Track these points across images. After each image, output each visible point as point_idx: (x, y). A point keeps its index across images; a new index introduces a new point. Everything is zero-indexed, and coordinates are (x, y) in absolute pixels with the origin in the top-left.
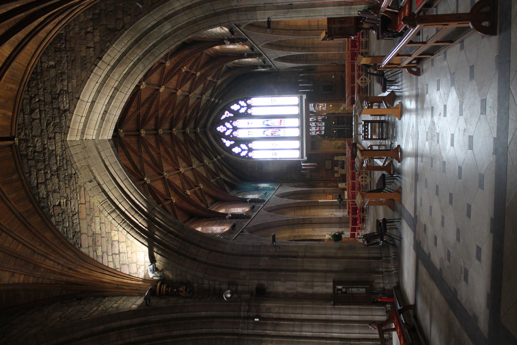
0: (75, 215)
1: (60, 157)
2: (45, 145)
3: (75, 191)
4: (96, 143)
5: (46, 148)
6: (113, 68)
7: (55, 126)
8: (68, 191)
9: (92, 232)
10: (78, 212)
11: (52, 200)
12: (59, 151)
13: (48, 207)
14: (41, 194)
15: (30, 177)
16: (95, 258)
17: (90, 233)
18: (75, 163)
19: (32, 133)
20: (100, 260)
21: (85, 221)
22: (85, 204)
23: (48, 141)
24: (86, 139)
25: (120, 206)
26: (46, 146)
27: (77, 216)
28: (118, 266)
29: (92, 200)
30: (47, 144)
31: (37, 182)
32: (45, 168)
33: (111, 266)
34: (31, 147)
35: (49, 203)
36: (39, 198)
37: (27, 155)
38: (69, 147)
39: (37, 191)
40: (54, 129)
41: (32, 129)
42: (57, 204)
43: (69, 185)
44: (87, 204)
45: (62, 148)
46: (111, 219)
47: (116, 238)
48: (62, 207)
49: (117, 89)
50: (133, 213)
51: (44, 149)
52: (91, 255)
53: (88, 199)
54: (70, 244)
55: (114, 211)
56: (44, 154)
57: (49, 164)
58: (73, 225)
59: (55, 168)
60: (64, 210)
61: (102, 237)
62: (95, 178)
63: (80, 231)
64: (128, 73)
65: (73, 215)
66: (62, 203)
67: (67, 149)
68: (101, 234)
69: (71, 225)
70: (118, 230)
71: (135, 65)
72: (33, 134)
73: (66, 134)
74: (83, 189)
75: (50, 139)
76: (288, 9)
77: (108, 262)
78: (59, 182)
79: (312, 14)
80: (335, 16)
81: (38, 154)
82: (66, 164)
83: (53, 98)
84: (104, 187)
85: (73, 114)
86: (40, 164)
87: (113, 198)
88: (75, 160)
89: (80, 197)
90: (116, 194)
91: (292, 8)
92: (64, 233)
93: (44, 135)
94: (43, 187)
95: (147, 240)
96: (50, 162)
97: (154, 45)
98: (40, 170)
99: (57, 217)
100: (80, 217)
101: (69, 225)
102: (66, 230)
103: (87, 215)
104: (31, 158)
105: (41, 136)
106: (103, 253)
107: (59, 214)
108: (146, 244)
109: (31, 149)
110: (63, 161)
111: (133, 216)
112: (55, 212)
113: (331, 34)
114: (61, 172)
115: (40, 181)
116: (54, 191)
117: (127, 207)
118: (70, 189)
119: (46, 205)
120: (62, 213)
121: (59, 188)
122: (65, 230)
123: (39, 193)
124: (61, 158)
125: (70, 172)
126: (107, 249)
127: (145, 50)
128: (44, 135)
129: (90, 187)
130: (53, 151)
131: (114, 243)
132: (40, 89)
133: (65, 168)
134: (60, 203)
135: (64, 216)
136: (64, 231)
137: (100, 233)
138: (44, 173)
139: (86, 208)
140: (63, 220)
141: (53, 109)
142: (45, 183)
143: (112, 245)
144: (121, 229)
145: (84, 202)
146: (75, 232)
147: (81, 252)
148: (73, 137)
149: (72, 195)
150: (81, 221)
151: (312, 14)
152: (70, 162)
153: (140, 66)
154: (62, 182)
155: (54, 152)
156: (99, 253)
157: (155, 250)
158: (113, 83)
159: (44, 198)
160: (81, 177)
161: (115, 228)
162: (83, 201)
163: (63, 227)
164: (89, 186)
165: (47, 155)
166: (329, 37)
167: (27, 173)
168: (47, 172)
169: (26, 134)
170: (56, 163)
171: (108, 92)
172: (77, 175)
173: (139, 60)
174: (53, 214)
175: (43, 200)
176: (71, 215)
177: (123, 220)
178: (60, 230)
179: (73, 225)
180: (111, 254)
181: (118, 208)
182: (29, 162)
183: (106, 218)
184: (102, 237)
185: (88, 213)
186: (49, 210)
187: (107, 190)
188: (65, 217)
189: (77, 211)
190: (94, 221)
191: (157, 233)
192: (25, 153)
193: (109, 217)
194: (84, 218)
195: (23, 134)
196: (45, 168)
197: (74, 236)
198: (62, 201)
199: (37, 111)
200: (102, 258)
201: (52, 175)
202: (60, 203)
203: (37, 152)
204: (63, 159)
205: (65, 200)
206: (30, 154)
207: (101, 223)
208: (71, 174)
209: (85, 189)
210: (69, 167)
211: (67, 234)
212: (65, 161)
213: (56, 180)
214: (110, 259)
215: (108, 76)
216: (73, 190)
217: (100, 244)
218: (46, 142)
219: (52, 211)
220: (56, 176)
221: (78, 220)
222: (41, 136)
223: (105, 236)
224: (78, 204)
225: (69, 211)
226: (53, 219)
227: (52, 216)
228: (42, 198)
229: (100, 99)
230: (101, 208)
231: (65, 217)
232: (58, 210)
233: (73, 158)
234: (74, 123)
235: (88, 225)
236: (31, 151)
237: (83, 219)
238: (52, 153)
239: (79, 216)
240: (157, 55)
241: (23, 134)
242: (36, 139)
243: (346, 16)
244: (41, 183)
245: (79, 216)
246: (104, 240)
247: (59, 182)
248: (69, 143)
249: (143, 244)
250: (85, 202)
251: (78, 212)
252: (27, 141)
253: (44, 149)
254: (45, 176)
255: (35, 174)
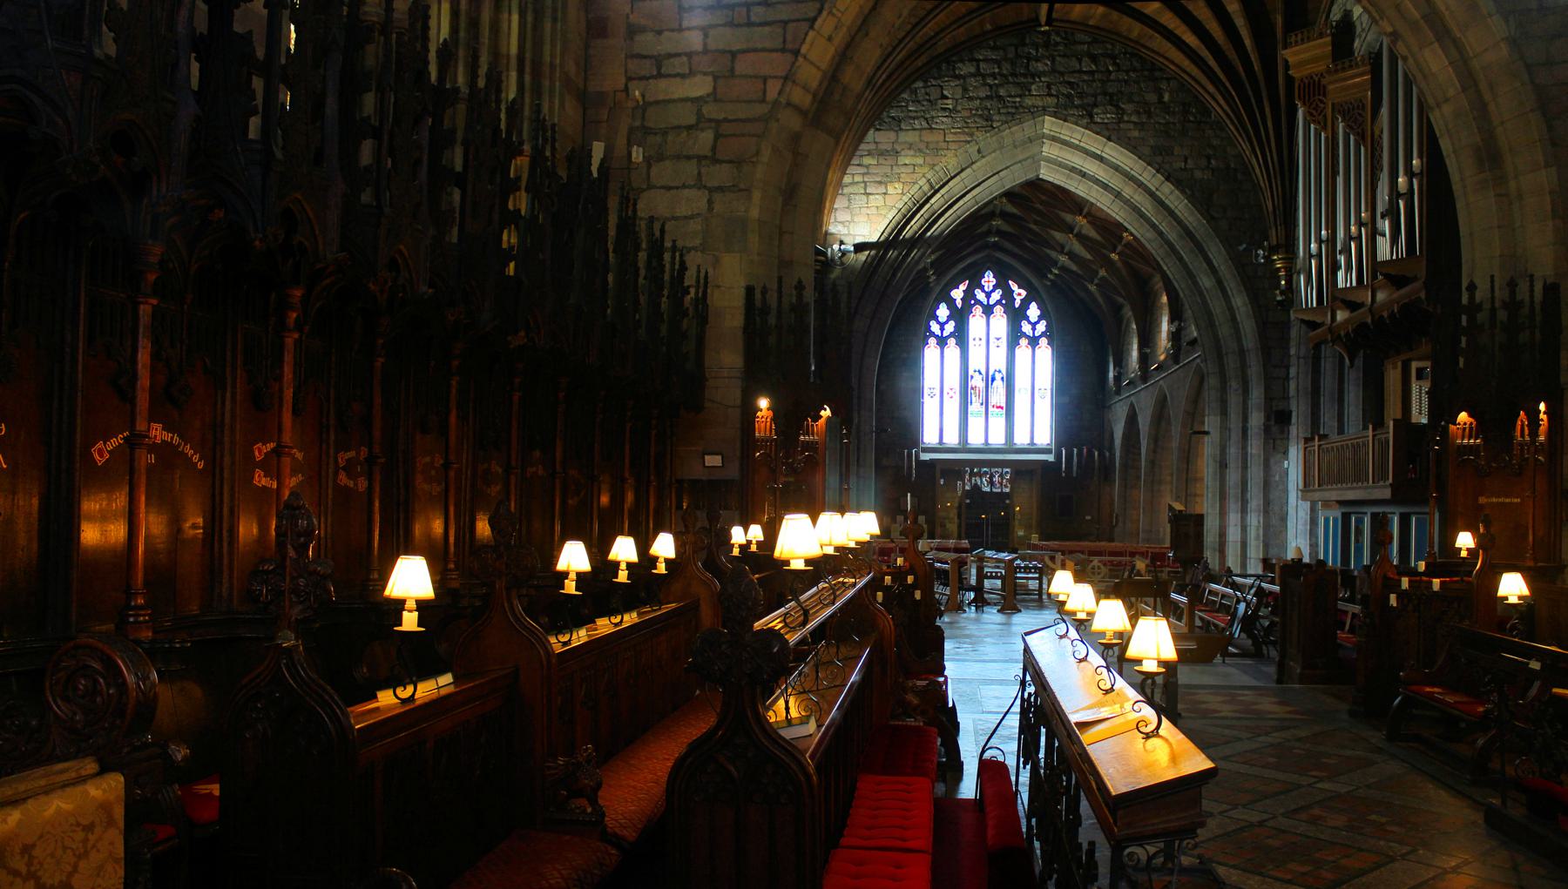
0: (928, 123)
1: (1019, 102)
2: (1039, 78)
3: (965, 125)
4: (1036, 160)
5: (1034, 79)
6: (1152, 194)
7: (1069, 96)
8: (966, 114)
9: (899, 150)
10: (931, 128)
11: (952, 84)
12: (1028, 101)
13: (940, 77)
14: (960, 65)
15: (989, 48)
16: (858, 153)
17: (898, 148)
18: (1010, 128)
19: (1060, 56)
20: (854, 161)
21: (917, 139)
22: (945, 141)
23: (1045, 84)
24: (1043, 143)
25: (938, 195)
26: (1037, 80)
27: (925, 124)
28: (846, 191)
29: (950, 154)
30: (1041, 81)
31: (981, 60)
32: (1002, 75)
33: (847, 179)
34: (1037, 53)
35: (946, 79)
36: (954, 62)
37: (1024, 45)
38: (1034, 118)
39: (966, 58)
40: (1063, 94)
41: (1064, 56)
42: (945, 93)
43: (975, 115)
44: (944, 145)
45: (1034, 107)
46: (921, 183)
47: (891, 190)
48: (940, 101)
49: (1118, 195)
50: (926, 216)
51: (1033, 76)
52: (863, 146)
53: (952, 146)
54: (881, 113)
55: (932, 187)
56: (1025, 76)
57: (1008, 83)
58: (911, 118)
59: (1002, 92)
60: (936, 104)
61: (892, 166)
62: (983, 157)
63: (901, 129)
64: (1142, 215)
65: (926, 119)
66: (946, 101)
67: (1031, 117)
68: (897, 165)
69: (910, 114)
70: (903, 194)
71: (1153, 226)
72: (1058, 58)
73: (1055, 115)
74: (969, 139)
75: (1049, 87)
76: (1220, 462)
77: (853, 175)
78: (980, 99)
79: (1210, 495)
80: (1205, 527)
81: (1024, 65)
82: (1009, 113)
83: (1111, 95)
84: (969, 171)
85: (1086, 128)
86: (1009, 67)
87: (951, 184)
88: (1014, 129)
89: (955, 133)
90: (956, 190)
91: (1221, 466)
92: (898, 102)
93: (1055, 77)
94: (972, 70)
95: (887, 238)
96: (1011, 85)
97: (1181, 259)
98: (999, 67)
99: (923, 91)
100: (924, 132)
101: (911, 111)
102: (902, 106)
103: (927, 143)
104: (1019, 51)
105: (1054, 71)
106: (867, 167)
107: (929, 96)
108: (881, 239)
109: (1034, 52)
110: (1012, 107)
111: (922, 215)
112: (932, 88)
113: (1177, 519)
114: (995, 102)
115: (982, 65)
116: (965, 90)
117: (935, 207)
118: (968, 118)
119: (943, 73)
120: (929, 101)
121: (971, 99)
122: (903, 104)
123: (962, 61)
124: (1018, 104)
125: (996, 117)
126: (874, 174)
127: (1175, 244)
128: (1055, 77)
129: (970, 150)
130: (1030, 91)
131: (883, 186)
132: (1127, 75)
133: (1001, 111)
134: (947, 98)
135: (925, 103)
136: (901, 102)
137: (900, 163)
138: (994, 73)
139: (937, 142)
140: (919, 102)
141: (1095, 96)
142: (978, 74)
143: (880, 183)
144: (905, 199)
145: (947, 139)
146: (900, 121)
147: (868, 130)
148: (1049, 124)
149: (958, 119)
150: (917, 133)
151: (1210, 495)
152: (1010, 118)
153: (1151, 234)
154: (980, 104)
155: (1027, 93)
156: (867, 161)
157: (873, 252)
158: (1128, 191)
159: (954, 70)
160: (987, 137)
161: (906, 189)
162: (950, 138)
163: (908, 101)
164: (973, 149)
165: (1023, 80)
166: (1175, 516)
167: (994, 43)
168: (995, 79)
169: (1057, 44)
170: (1010, 96)
171: (1116, 182)
172: (989, 131)
173: (1161, 234)
174: (929, 84)
175: (951, 67)
176: (928, 116)
177: (918, 202)
178: (905, 96)
179: (911, 118)
180: (866, 180)
181: (937, 191)
182: (1013, 49)
183: (921, 175)
184: (892, 166)
185: (931, 146)
186: (935, 78)
187: (963, 175)
188: (923, 106)
189: (933, 126)
190: (918, 154)
191: (896, 253)
192: (1027, 41)
193: (924, 180)
194: (922, 138)
195: (1058, 39)
196: (1002, 75)
197: (893, 118)
198: (949, 101)
199: (1094, 67)
200: (858, 165)
201: (991, 86)
202: (947, 98)
203: (1028, 63)
204: (1016, 108)
205: (950, 107)
206: (1026, 50)
207: (914, 165)
208: (992, 121)
209: (968, 142)
210: (1003, 118)
211: (897, 107)
212: (1013, 111)
213: (982, 95)
214: (857, 179)
215: (1140, 185)
216: (966, 122)
217: (880, 162)
218: (1043, 79)
219: (934, 83)
220: (989, 93)
221: (918, 127)
222: (1054, 71)
223: (894, 172)
224: (944, 130)
225: (933, 113)
226: (919, 84)
227: (925, 81)
228: (954, 66)
229: (1104, 170)
230: (937, 168)
231: (923, 106)
232: (935, 94)
233: (1017, 124)
234: (1071, 128)
235: (911, 144)
236: (1030, 53)
237: (920, 136)
238: (1025, 90)
239: (925, 129)
240: (1167, 261)
241: (1058, 39)
242: (1049, 63)
243: (1205, 543)
244: (978, 66)
245: (925, 129)
246: (888, 170)
247: (980, 99)
248: (1040, 118)
249: (882, 234)
250: (948, 142)
251: (931, 128)
252: (1047, 45)
253: (1033, 76)
254: (988, 75)
255: (994, 57)
